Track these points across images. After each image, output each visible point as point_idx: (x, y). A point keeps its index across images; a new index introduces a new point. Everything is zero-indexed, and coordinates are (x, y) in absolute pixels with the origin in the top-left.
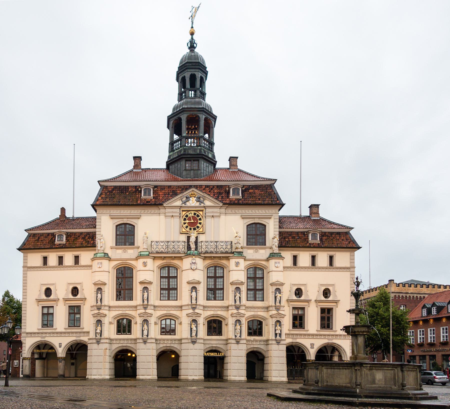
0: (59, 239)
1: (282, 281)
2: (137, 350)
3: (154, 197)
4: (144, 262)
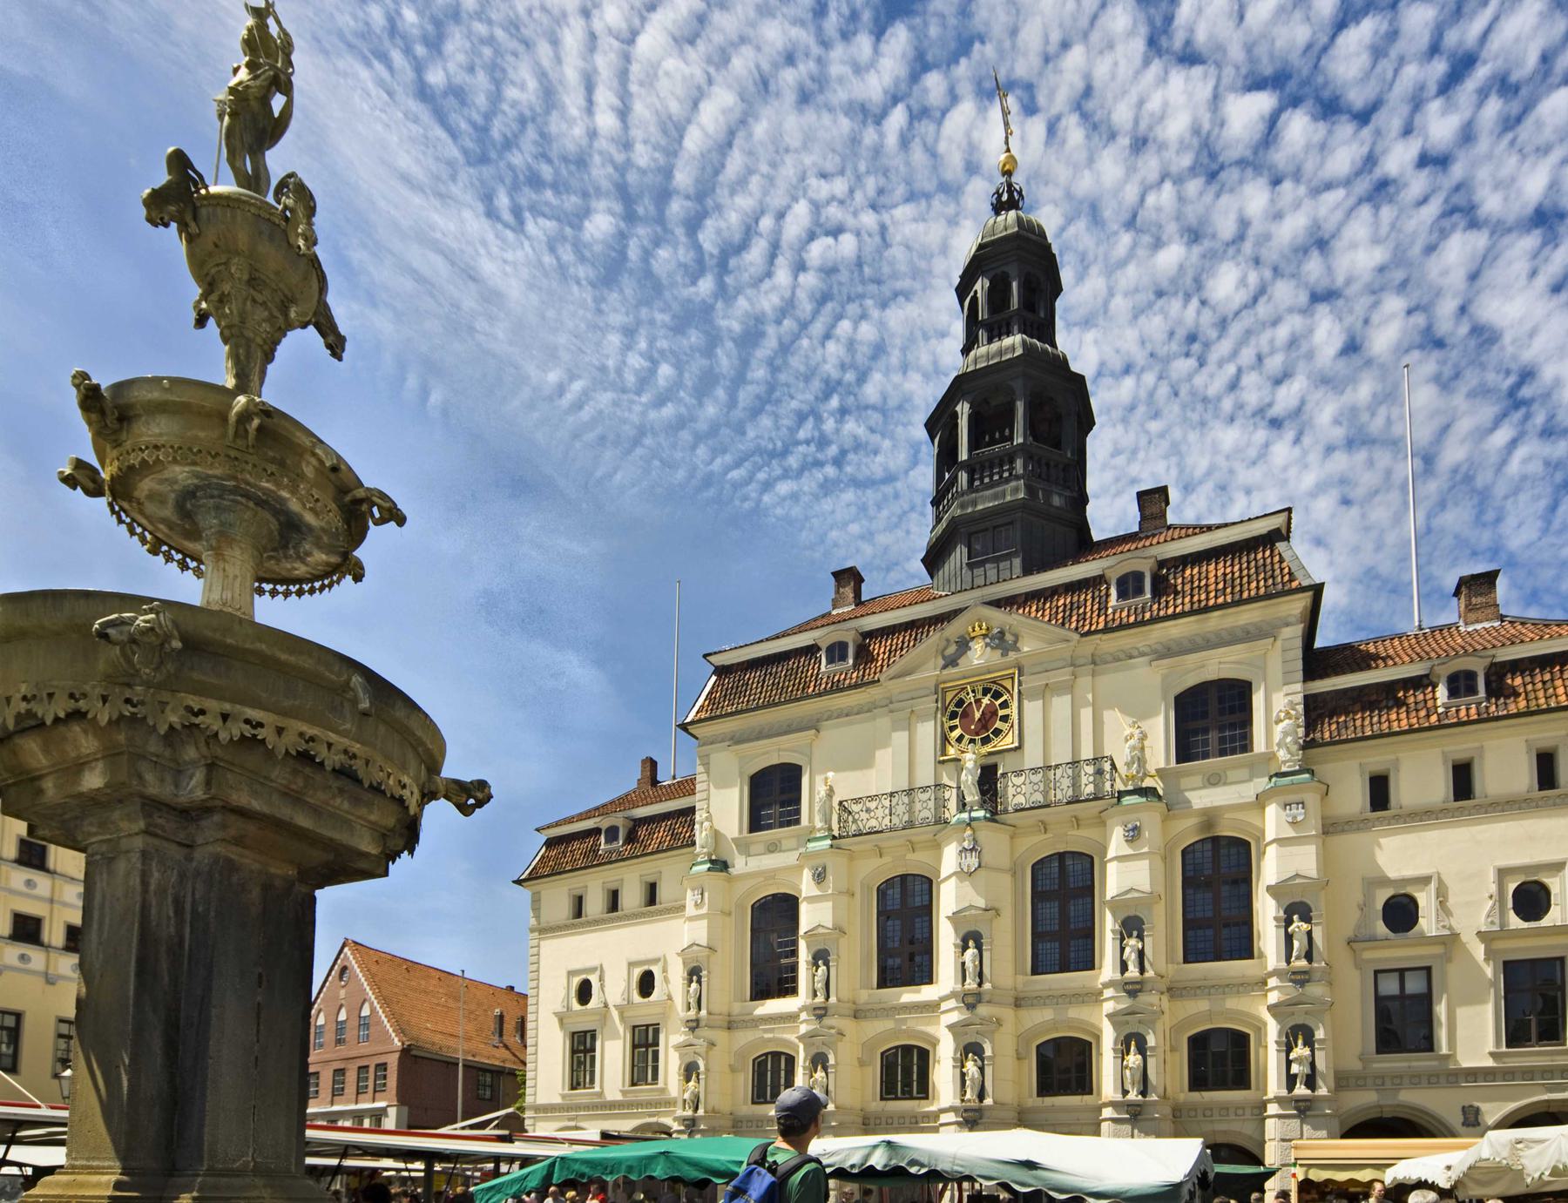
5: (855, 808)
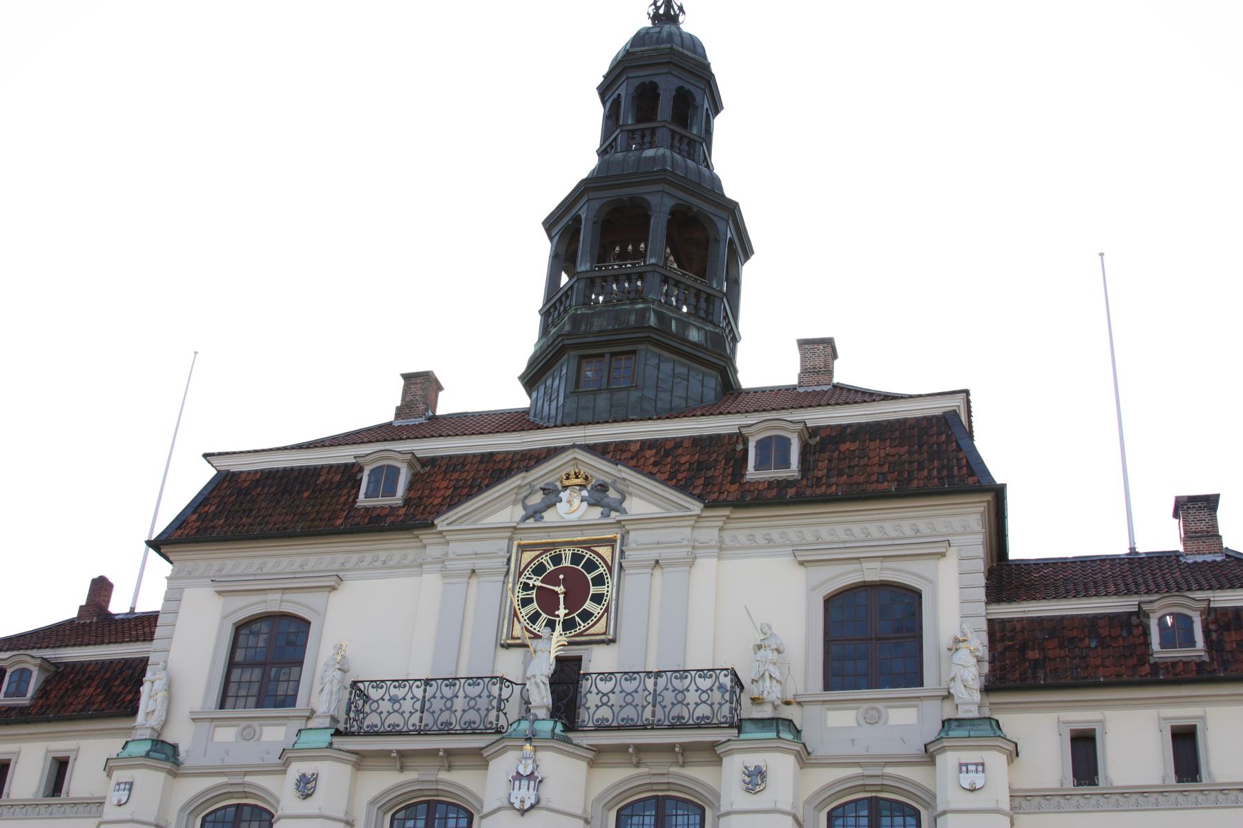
3: (407, 501)
5: (374, 694)
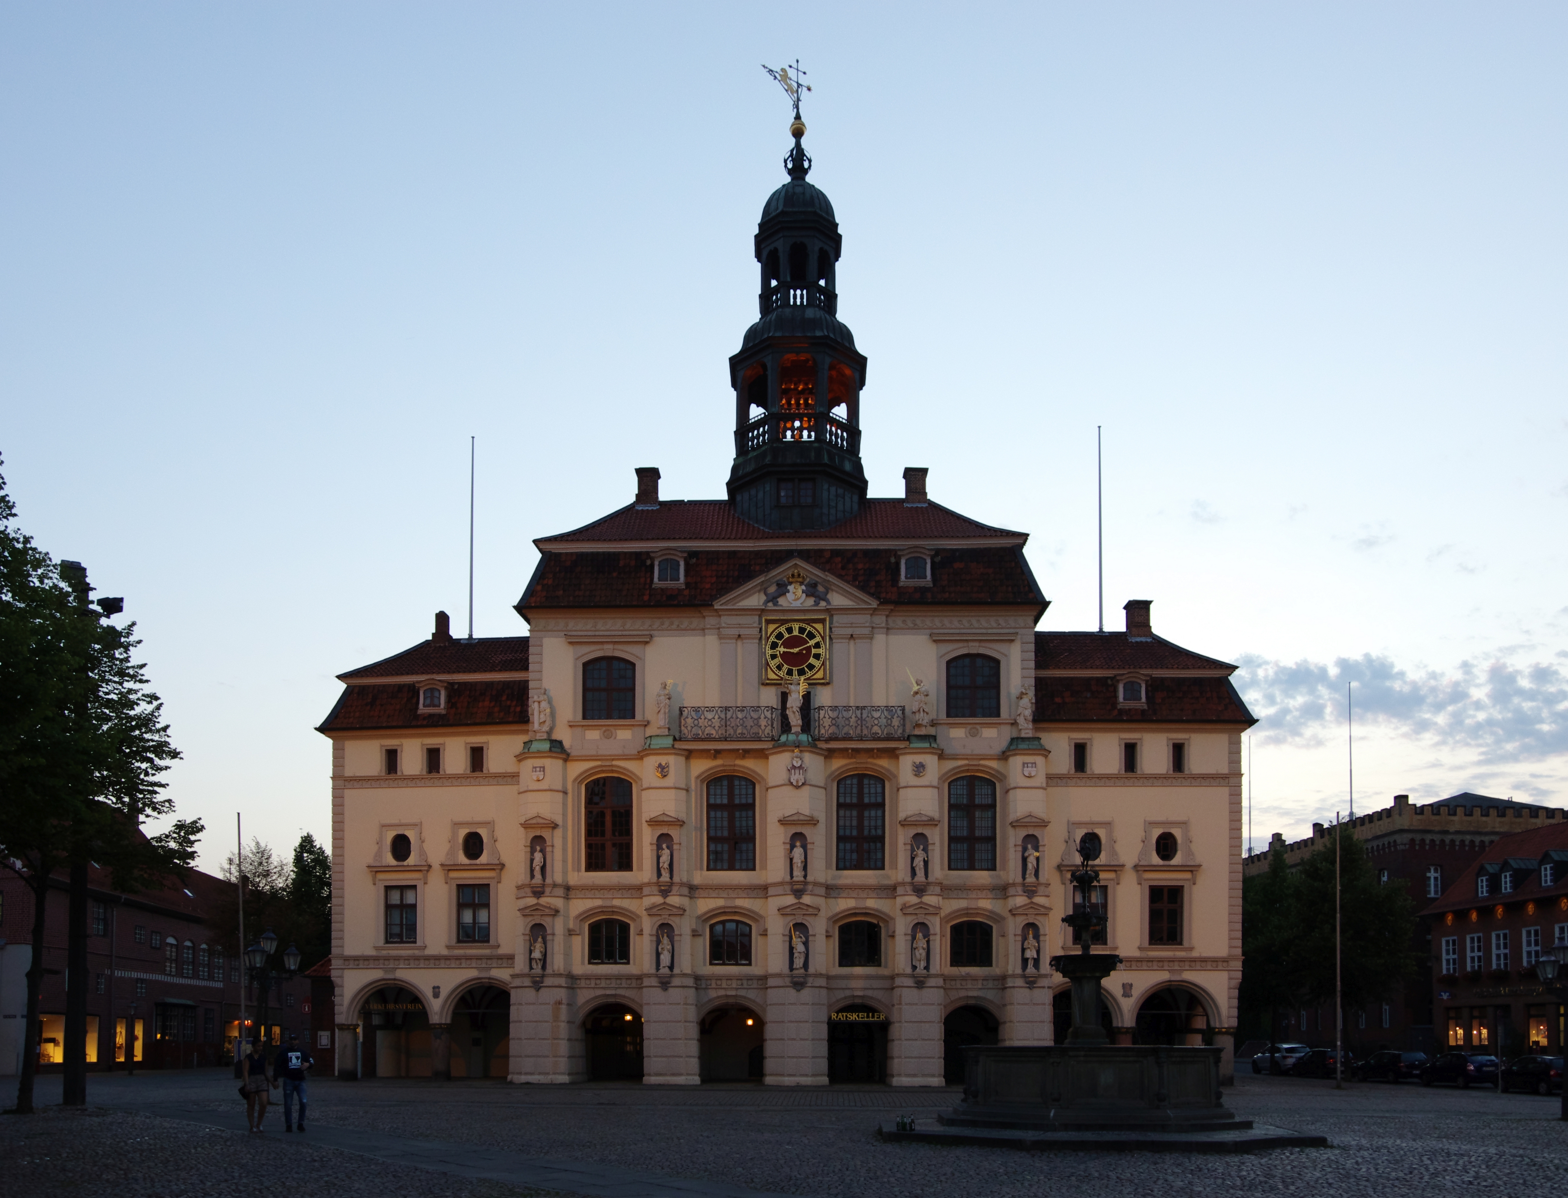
0: (428, 702)
1: (1043, 815)
2: (645, 1007)
3: (687, 584)
4: (660, 765)
